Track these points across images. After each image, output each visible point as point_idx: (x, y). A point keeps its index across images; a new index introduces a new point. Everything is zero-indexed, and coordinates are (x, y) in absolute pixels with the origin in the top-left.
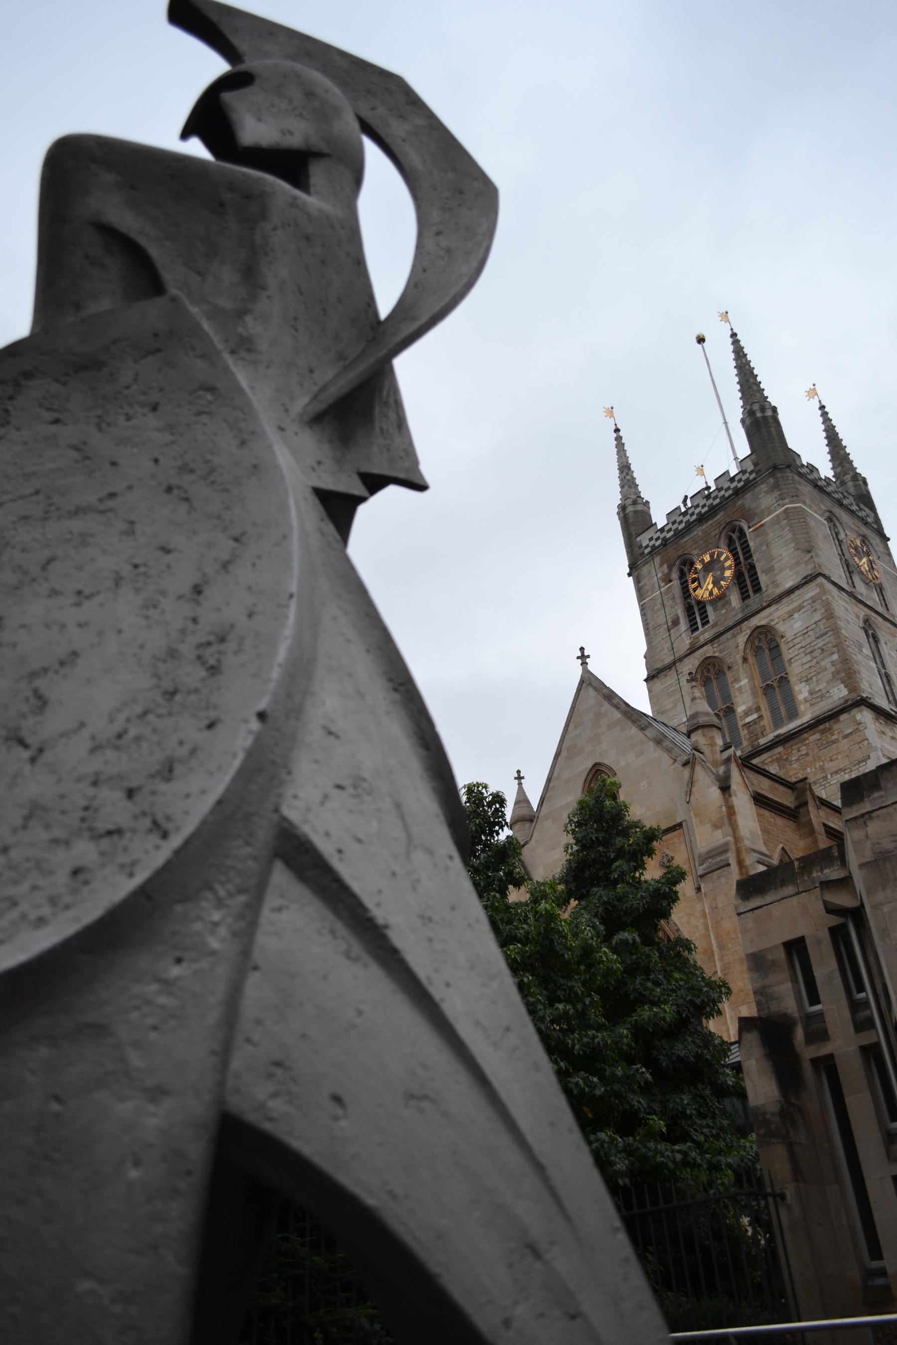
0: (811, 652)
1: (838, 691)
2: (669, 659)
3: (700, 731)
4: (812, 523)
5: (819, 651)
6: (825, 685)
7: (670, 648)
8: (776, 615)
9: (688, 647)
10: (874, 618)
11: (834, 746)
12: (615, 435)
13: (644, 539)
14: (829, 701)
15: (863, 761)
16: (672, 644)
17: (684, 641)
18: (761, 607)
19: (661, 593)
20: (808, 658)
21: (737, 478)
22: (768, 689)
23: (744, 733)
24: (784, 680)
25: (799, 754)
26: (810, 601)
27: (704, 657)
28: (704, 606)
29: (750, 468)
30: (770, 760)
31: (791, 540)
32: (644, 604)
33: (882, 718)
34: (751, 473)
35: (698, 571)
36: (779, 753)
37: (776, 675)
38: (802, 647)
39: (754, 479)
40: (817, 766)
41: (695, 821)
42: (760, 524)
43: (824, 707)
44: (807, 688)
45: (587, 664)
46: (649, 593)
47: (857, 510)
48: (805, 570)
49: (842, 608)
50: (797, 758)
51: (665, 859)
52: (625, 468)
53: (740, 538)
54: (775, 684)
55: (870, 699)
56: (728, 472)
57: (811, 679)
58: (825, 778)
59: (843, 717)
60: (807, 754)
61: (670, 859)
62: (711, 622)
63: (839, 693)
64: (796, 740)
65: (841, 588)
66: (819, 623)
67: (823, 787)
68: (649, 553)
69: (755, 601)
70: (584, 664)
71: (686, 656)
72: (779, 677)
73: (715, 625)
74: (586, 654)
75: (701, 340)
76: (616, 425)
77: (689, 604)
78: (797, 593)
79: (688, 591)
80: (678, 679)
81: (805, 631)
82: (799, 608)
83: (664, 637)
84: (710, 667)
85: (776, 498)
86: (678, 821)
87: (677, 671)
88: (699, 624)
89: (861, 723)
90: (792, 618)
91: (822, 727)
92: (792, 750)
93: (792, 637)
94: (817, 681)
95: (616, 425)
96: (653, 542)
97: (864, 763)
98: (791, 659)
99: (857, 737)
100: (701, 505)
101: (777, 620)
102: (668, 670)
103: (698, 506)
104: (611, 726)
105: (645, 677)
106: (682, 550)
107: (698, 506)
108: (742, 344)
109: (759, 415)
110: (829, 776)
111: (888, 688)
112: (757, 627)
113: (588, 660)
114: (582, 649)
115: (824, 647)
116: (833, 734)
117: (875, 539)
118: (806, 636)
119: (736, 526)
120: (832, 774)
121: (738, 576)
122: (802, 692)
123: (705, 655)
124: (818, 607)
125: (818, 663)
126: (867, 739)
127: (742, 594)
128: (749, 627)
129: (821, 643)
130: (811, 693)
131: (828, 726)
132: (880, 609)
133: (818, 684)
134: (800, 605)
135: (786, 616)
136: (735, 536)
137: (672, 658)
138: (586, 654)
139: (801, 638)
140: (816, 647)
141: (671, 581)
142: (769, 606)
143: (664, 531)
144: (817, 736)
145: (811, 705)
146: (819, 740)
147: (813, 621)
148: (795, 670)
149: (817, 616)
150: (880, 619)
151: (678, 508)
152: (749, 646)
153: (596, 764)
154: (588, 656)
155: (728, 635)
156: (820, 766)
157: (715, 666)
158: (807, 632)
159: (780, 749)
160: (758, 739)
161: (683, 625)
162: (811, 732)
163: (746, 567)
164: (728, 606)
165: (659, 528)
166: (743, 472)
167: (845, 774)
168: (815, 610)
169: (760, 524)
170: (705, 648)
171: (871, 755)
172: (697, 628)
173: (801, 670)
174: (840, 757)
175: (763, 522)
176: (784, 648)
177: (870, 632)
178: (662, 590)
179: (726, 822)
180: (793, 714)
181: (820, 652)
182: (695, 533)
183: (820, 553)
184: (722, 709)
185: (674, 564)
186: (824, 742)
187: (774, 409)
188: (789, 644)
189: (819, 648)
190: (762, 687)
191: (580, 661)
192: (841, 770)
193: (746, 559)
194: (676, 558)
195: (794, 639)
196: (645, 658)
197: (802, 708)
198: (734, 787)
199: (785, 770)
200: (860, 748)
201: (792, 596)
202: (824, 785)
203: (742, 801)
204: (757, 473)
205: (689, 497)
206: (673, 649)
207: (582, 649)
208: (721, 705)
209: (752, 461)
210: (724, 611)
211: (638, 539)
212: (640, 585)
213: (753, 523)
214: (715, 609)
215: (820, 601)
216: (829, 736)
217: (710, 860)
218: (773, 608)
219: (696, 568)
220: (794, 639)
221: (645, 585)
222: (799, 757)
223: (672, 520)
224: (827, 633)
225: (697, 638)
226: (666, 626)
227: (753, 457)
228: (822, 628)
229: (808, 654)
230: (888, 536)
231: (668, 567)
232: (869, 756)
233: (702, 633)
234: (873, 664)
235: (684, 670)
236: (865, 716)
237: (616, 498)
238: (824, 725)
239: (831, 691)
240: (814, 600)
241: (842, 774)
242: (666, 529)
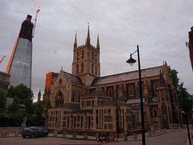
4: (90, 53)
13: (75, 48)
17: (77, 61)
24: (83, 69)
43: (85, 73)
48: (88, 59)
52: (76, 39)
63: (87, 72)
65: (90, 61)
69: (83, 60)
75: (88, 23)
121: (82, 56)
122: (84, 71)
132: (95, 62)
148: (84, 68)
161: (77, 60)
180: (83, 73)
187: (90, 39)
203: (71, 86)
236: (88, 75)
237: (74, 42)
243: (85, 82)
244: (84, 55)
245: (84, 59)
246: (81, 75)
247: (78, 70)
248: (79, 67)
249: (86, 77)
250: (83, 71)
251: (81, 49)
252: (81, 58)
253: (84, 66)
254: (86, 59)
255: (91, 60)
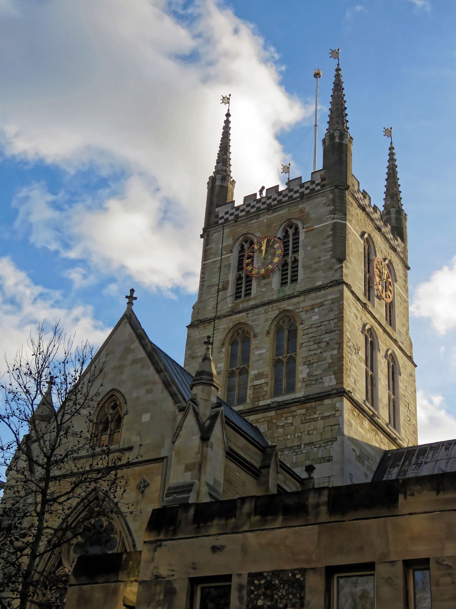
0: (319, 343)
1: (329, 380)
2: (212, 315)
3: (200, 387)
5: (325, 343)
6: (321, 372)
7: (215, 306)
8: (302, 305)
9: (229, 309)
10: (377, 329)
11: (313, 423)
12: (225, 118)
13: (221, 211)
14: (321, 386)
15: (330, 441)
16: (217, 304)
18: (292, 295)
19: (221, 260)
20: (316, 346)
21: (306, 185)
22: (277, 363)
23: (250, 392)
24: (292, 360)
25: (286, 421)
26: (330, 302)
27: (238, 322)
28: (251, 281)
29: (318, 181)
30: (263, 420)
31: (331, 249)
32: (206, 264)
33: (357, 410)
34: (317, 185)
35: (255, 250)
36: (271, 417)
37: (288, 353)
38: (313, 337)
39: (319, 190)
40: (296, 435)
41: (174, 460)
42: (312, 228)
43: (316, 389)
44: (308, 370)
45: (133, 304)
46: (212, 256)
47: (391, 239)
49: (353, 315)
50: (283, 424)
51: (142, 484)
53: (294, 234)
54: (285, 360)
55: (351, 393)
56: (300, 178)
57: (313, 364)
58: (300, 446)
59: (327, 402)
60: (292, 424)
61: (146, 485)
62: (252, 295)
64: (286, 410)
66: (331, 322)
67: (296, 453)
68: (222, 224)
69: (289, 290)
70: (130, 303)
71: (225, 316)
72: (289, 355)
73: (255, 298)
74: (134, 295)
76: (229, 110)
77: (240, 275)
78: (323, 292)
79: (242, 264)
80: (213, 334)
81: (319, 325)
82: (321, 305)
83: (213, 296)
84: (240, 331)
85: (330, 211)
86: (162, 455)
87: (214, 327)
88: (243, 294)
89: (338, 411)
90: (313, 311)
91: (309, 405)
92: (282, 417)
93: (308, 327)
94: (317, 367)
95: (229, 110)
96: (227, 216)
97: (331, 443)
98: (303, 343)
99: (332, 421)
100: (273, 198)
101: (301, 309)
102: (208, 324)
103: (270, 198)
104: (134, 362)
105: (189, 324)
106: (248, 230)
107: (270, 198)
108: (342, 79)
109: (337, 140)
110: (302, 446)
111: (369, 387)
112: (285, 310)
113: (134, 301)
114: (132, 291)
115: (330, 342)
116: (315, 413)
117: (398, 265)
118: (319, 328)
119: (294, 224)
120: (305, 444)
121: (285, 264)
123: (239, 320)
124: (335, 308)
125: (321, 353)
126: (339, 424)
127: (282, 279)
128: (280, 309)
129: (327, 338)
130: (309, 375)
131: (313, 406)
132: (384, 323)
133: (316, 370)
134: (322, 303)
135: (309, 308)
136: (291, 232)
137: (213, 315)
138: (134, 295)
139: (315, 329)
140: (324, 340)
141: (231, 252)
142: (298, 296)
143: (239, 210)
144: (303, 411)
145: (306, 385)
146: (305, 414)
147: (328, 318)
149: (332, 315)
150: (381, 330)
151: (255, 195)
152: (275, 323)
153: (113, 390)
154: (136, 298)
155: (262, 309)
156: (298, 436)
157: (244, 331)
158: (321, 326)
159: (273, 413)
160: (259, 401)
161: (231, 290)
162: (300, 407)
163: (291, 260)
164: (268, 286)
165: (235, 206)
166: (312, 182)
167: (315, 447)
168: (332, 310)
169: (312, 228)
170: (241, 314)
171: (338, 438)
172: (240, 297)
173: (307, 355)
174: (315, 433)
175: (314, 227)
176: (300, 333)
177: (370, 339)
178: (223, 257)
179: (197, 466)
180: (291, 388)
181: (325, 345)
182: (261, 219)
183: (350, 266)
184: (239, 368)
185: (238, 239)
186: (307, 418)
188: (305, 331)
189: (325, 342)
190: (274, 359)
191: (127, 300)
192: (312, 443)
193: (294, 252)
194: (242, 234)
195: (309, 328)
196: (193, 308)
197: (299, 385)
198: (212, 439)
199: (271, 431)
200: (332, 430)
201: (318, 294)
202: (297, 452)
204: (321, 187)
205: (266, 188)
206: (217, 308)
207: (132, 291)
208: (239, 364)
209: (321, 176)
210: (264, 290)
211: (217, 210)
212: (208, 247)
213: (307, 225)
214: (258, 285)
215: (337, 304)
216: (312, 414)
217: (175, 495)
218: (302, 298)
219: (254, 248)
220: (309, 328)
221: (211, 249)
222: (285, 424)
223: (248, 203)
224: (334, 331)
225: (238, 305)
226: (217, 288)
227: (323, 172)
228: (333, 326)
229: (316, 343)
230: (409, 266)
231: (233, 240)
232: (336, 438)
233: (243, 302)
234: (363, 366)
235: (220, 327)
238: (311, 403)
239: (324, 378)
240: (333, 301)
241: (313, 447)
242: (241, 208)
243: (310, 469)
244: (301, 256)
245: (300, 286)
246: (268, 408)
247: (244, 371)
248: (254, 343)
249: (320, 424)
250: (292, 374)
251: (270, 208)
252: (276, 279)
253: (301, 339)
254: (319, 283)
255: (362, 297)
